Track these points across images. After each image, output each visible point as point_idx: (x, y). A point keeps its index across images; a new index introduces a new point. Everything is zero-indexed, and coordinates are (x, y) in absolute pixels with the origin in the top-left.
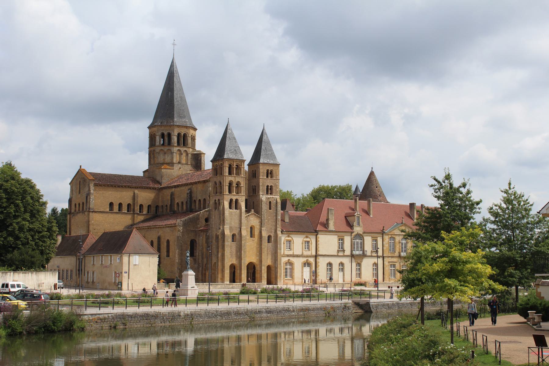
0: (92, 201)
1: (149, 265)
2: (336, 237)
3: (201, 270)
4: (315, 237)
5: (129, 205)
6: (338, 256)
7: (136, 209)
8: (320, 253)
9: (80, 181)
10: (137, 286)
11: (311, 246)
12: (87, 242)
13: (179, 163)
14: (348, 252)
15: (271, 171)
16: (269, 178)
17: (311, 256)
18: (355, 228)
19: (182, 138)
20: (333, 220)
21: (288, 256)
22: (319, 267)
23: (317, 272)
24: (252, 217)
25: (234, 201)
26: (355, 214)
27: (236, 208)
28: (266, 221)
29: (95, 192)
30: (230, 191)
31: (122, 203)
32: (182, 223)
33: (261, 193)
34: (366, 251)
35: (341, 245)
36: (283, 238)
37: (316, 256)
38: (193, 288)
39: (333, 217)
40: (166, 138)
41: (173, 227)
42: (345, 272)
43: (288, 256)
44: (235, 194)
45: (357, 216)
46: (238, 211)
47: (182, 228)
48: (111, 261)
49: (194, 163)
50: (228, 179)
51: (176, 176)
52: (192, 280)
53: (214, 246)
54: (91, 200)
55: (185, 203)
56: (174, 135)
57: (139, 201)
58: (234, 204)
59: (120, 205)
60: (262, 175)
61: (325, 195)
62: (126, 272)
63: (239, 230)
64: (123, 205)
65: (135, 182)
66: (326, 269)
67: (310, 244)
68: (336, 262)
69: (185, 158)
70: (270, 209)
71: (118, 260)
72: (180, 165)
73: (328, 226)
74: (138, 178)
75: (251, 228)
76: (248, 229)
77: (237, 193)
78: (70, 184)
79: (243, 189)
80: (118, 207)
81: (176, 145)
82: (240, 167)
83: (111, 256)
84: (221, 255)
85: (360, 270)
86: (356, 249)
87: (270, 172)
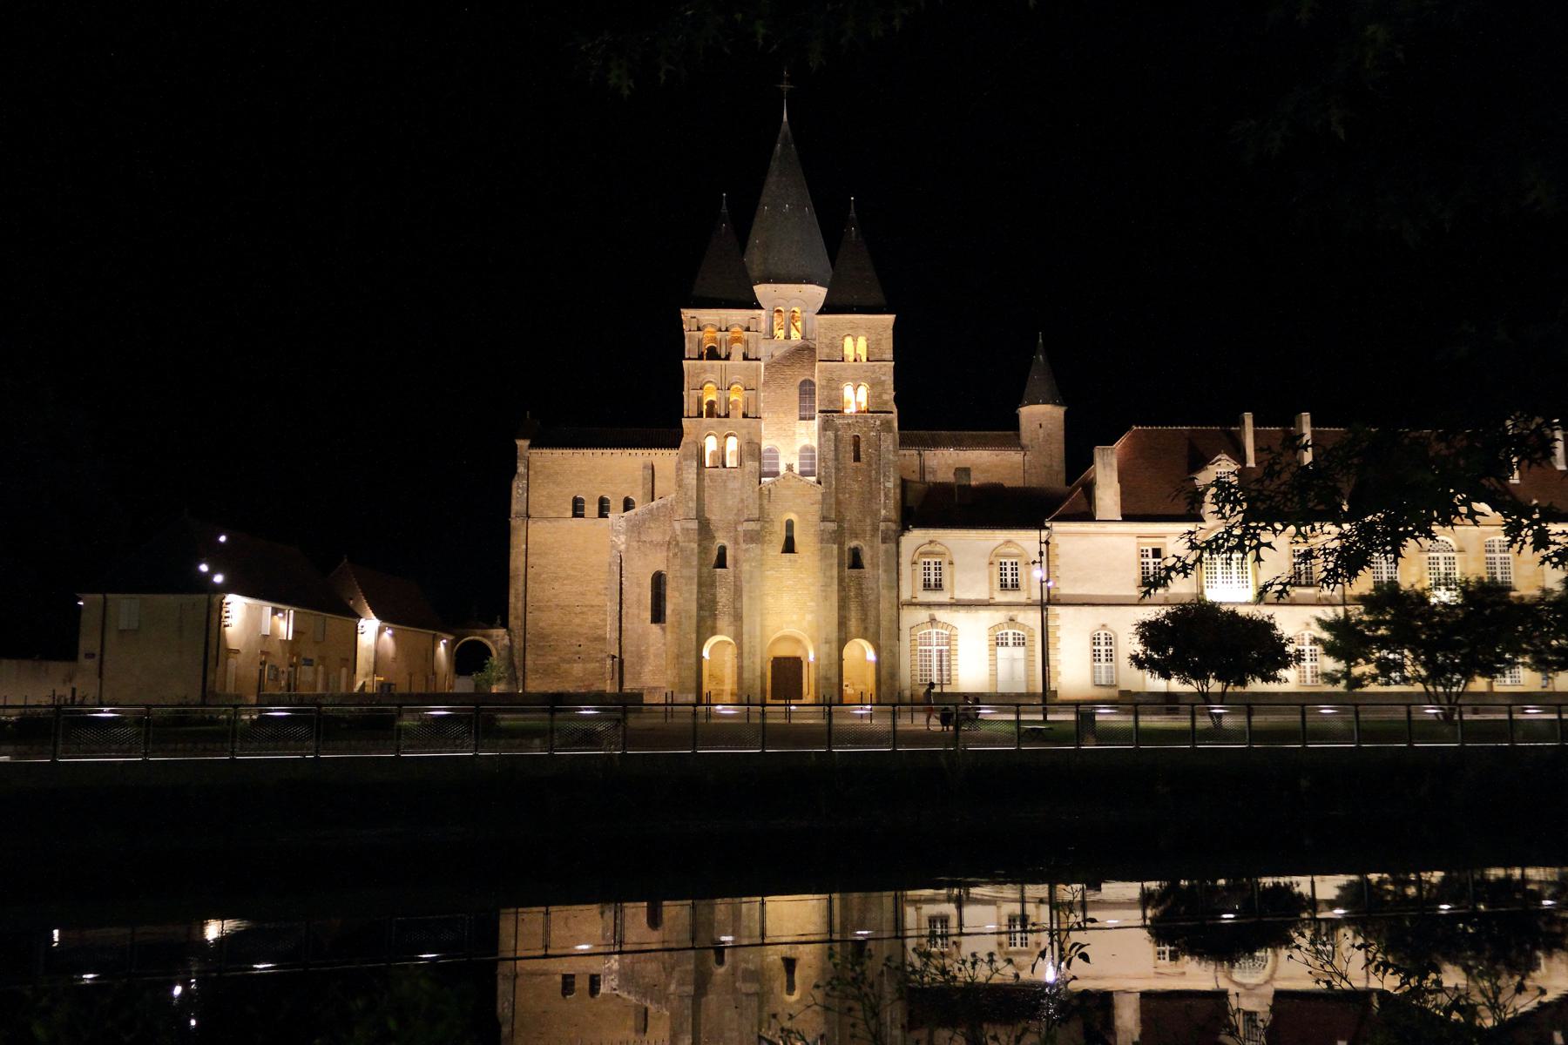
0: (523, 493)
20: (1115, 487)
21: (929, 605)
32: (623, 524)
43: (929, 605)
47: (623, 538)
61: (828, 342)
62: (90, 656)
66: (1088, 656)
84: (673, 611)
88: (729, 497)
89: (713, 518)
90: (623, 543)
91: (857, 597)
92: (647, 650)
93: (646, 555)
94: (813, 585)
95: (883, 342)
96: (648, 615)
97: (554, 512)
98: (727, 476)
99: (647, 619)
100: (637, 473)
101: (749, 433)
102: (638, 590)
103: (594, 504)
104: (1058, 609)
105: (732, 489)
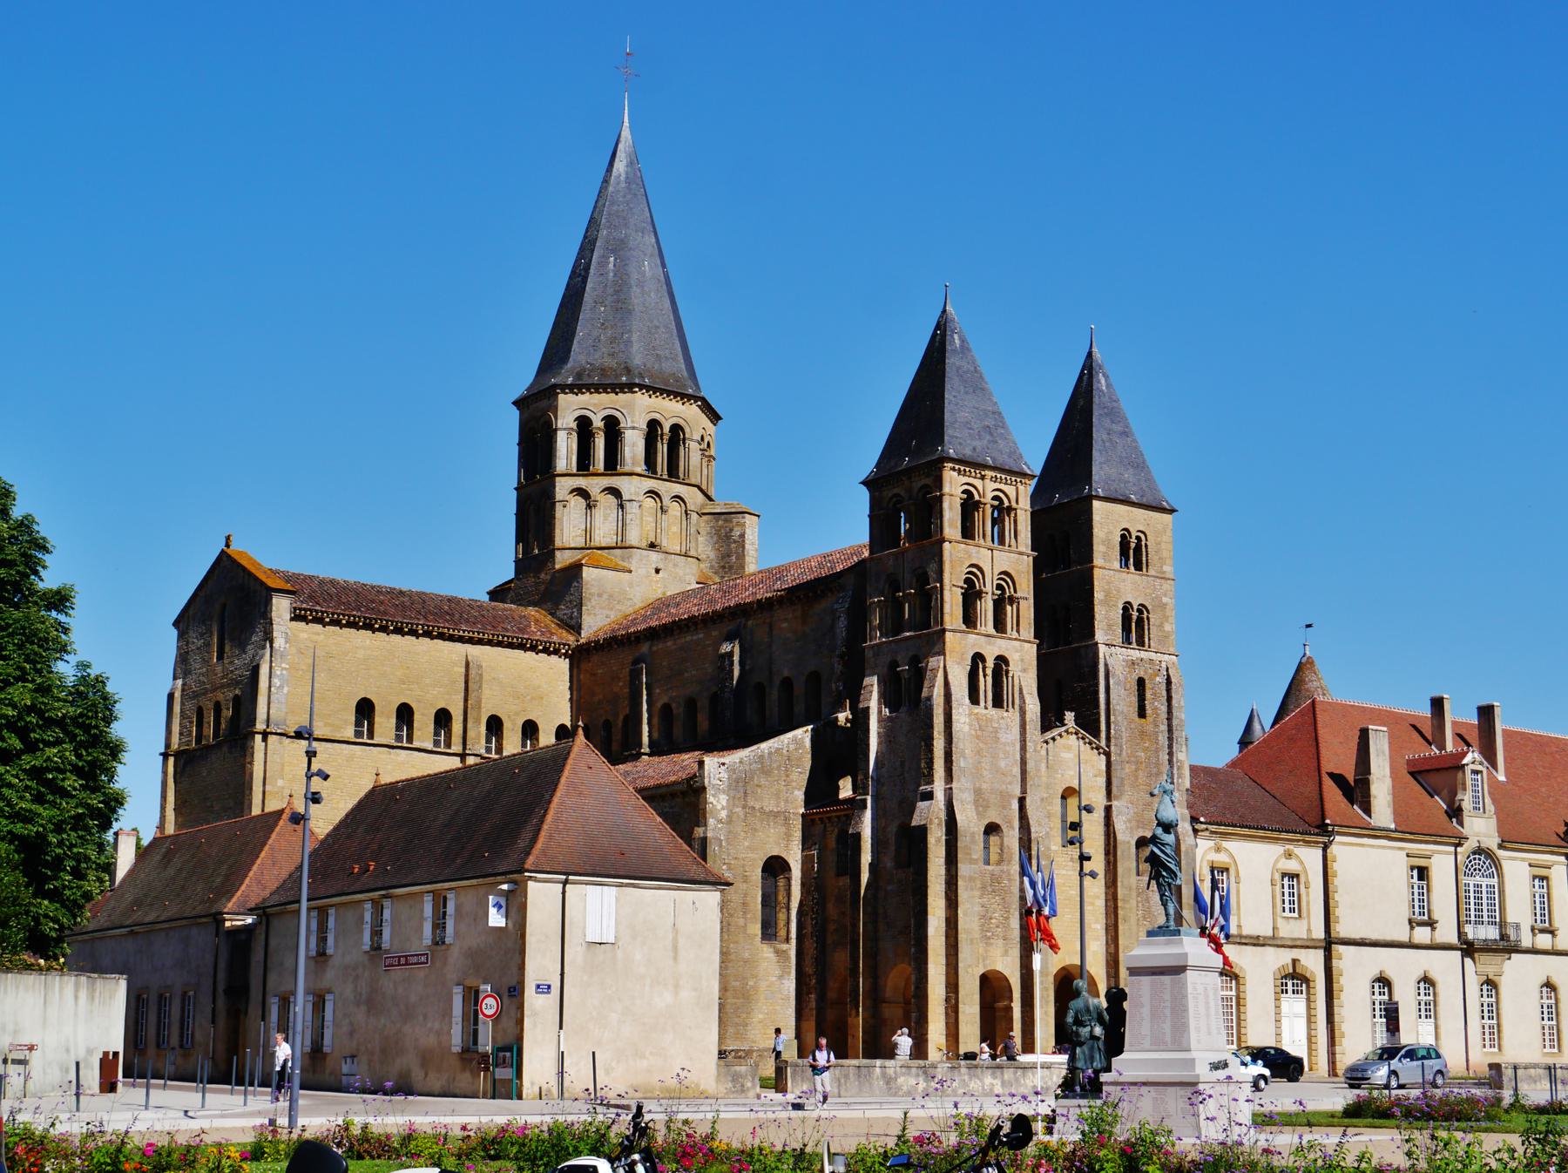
0: (281, 687)
1: (675, 948)
2: (1404, 853)
3: (813, 1004)
4: (1317, 853)
5: (442, 719)
6: (1411, 945)
7: (470, 734)
8: (1342, 929)
9: (224, 606)
10: (607, 1072)
11: (1308, 894)
12: (271, 849)
13: (652, 546)
14: (1446, 932)
15: (1138, 538)
16: (1132, 568)
17: (1308, 945)
18: (1466, 820)
19: (666, 438)
20: (1388, 782)
22: (1343, 996)
23: (1337, 1018)
24: (1069, 748)
25: (990, 664)
26: (1464, 762)
27: (998, 702)
28: (1128, 769)
29: (294, 650)
30: (970, 619)
31: (413, 705)
32: (724, 775)
33: (1100, 636)
34: (1517, 926)
35: (1416, 896)
36: (1202, 852)
37: (1328, 944)
38: (1221, 1074)
39: (1388, 774)
40: (600, 443)
41: (679, 800)
42: (1441, 1022)
44: (992, 631)
45: (1472, 767)
46: (1011, 717)
47: (723, 799)
48: (439, 925)
49: (712, 555)
50: (957, 556)
51: (642, 605)
52: (1207, 1008)
53: (889, 888)
54: (276, 681)
55: (703, 704)
56: (634, 428)
57: (483, 701)
58: (989, 679)
59: (405, 714)
60: (1105, 556)
62: (542, 989)
63: (1015, 805)
64: (416, 717)
65: (467, 621)
67: (1302, 886)
68: (1404, 968)
69: (675, 529)
70: (1142, 713)
71: (492, 911)
72: (654, 556)
73: (1368, 811)
74: (473, 604)
75: (1064, 797)
76: (1050, 804)
77: (1000, 625)
78: (176, 624)
79: (1028, 609)
80: (393, 721)
81: (641, 468)
82: (1010, 509)
83: (440, 902)
85: (1493, 1011)
86: (1473, 918)
87: (1134, 537)
88: (1002, 756)
89: (984, 786)
90: (723, 808)
91: (1145, 919)
92: (755, 988)
93: (756, 830)
94: (1098, 897)
95: (1163, 546)
96: (756, 929)
97: (326, 724)
98: (998, 722)
99: (756, 935)
100: (456, 669)
101: (1022, 660)
102: (745, 885)
103: (389, 717)
104: (1341, 949)
105: (1005, 744)
